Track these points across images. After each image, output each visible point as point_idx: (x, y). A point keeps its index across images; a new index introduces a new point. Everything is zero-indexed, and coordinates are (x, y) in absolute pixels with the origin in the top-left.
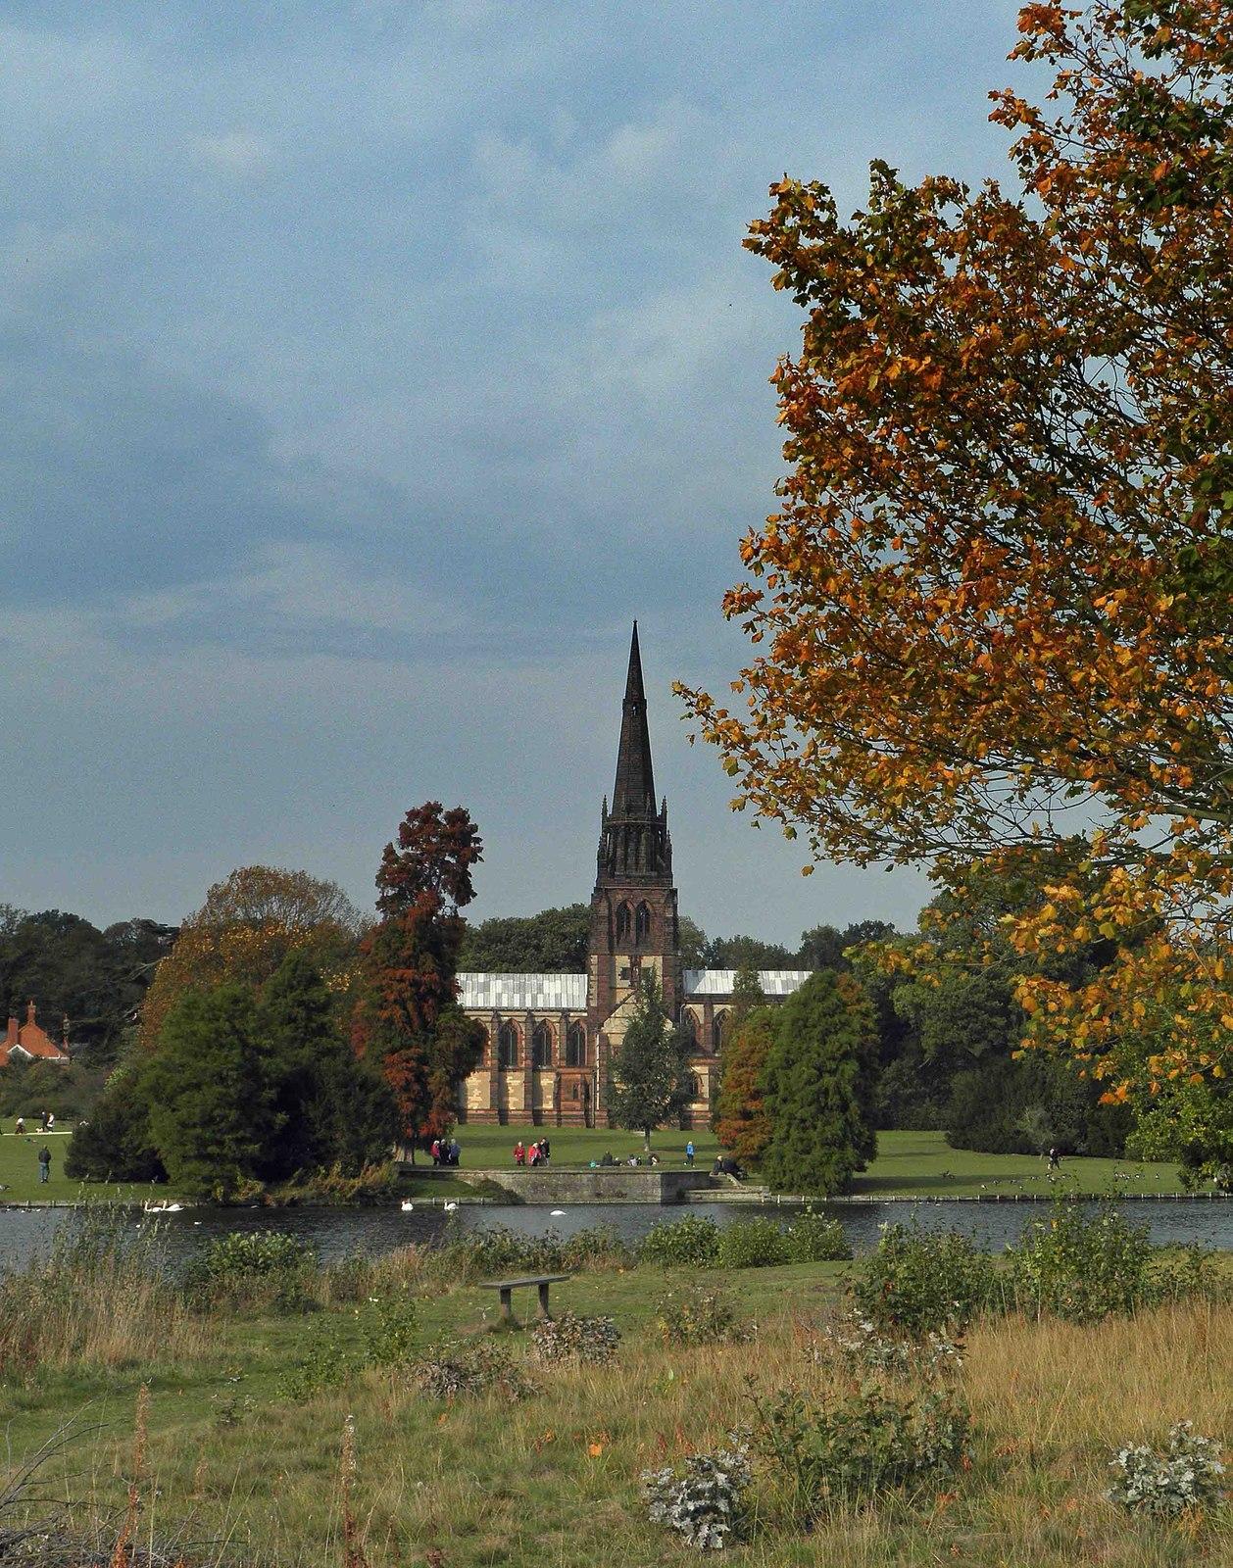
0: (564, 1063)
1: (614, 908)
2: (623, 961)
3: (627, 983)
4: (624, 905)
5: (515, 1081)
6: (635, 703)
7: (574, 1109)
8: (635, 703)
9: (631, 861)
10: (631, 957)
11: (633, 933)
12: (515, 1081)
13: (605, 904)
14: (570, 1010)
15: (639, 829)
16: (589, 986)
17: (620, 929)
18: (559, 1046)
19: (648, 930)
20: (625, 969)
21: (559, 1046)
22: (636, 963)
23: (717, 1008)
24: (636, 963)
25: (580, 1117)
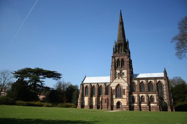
0: (104, 95)
1: (116, 60)
2: (118, 72)
4: (118, 59)
5: (94, 99)
6: (122, 23)
7: (105, 105)
8: (122, 23)
9: (120, 51)
10: (120, 70)
11: (121, 66)
12: (94, 99)
13: (114, 59)
14: (106, 83)
15: (122, 44)
16: (111, 77)
17: (118, 65)
18: (104, 91)
19: (124, 65)
20: (118, 73)
21: (104, 91)
22: (121, 72)
23: (141, 81)
24: (121, 72)
25: (106, 107)
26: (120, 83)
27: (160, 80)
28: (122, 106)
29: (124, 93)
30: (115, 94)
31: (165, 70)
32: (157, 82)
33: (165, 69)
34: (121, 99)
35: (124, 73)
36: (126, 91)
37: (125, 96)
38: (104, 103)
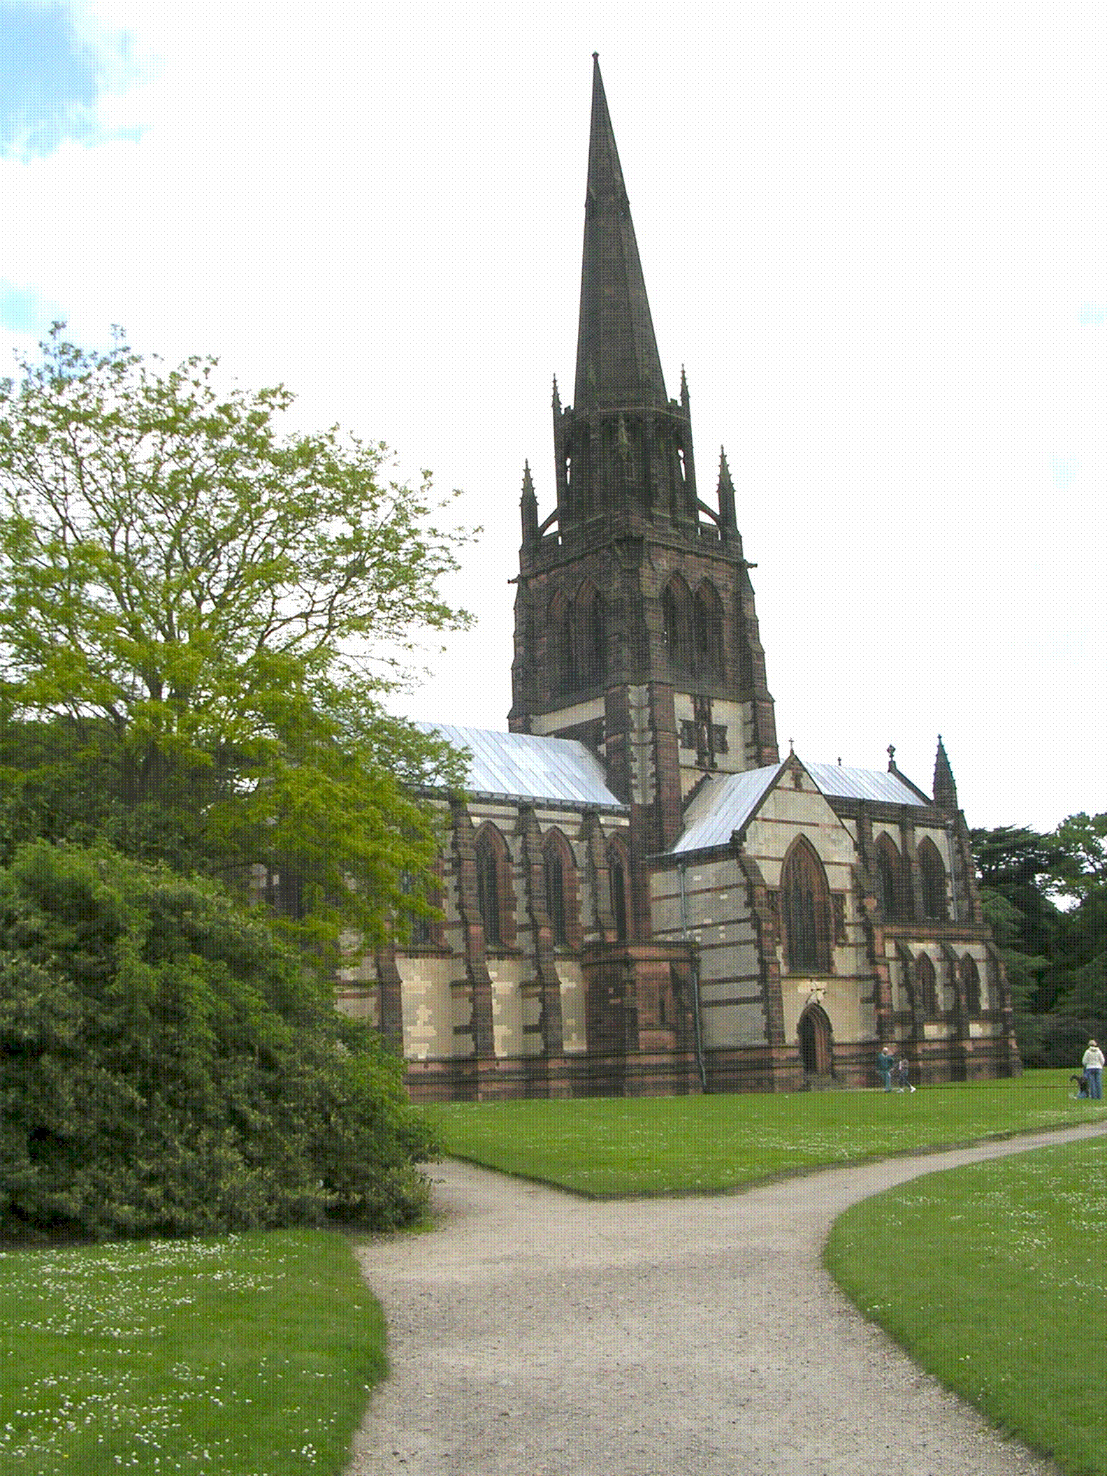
3: (688, 757)
5: (503, 980)
10: (695, 698)
20: (686, 724)
22: (703, 715)
26: (809, 832)
27: (929, 832)
28: (831, 1044)
29: (840, 924)
30: (784, 933)
31: (941, 746)
32: (918, 841)
33: (941, 746)
34: (822, 984)
35: (722, 729)
36: (849, 909)
37: (845, 960)
38: (650, 1026)
